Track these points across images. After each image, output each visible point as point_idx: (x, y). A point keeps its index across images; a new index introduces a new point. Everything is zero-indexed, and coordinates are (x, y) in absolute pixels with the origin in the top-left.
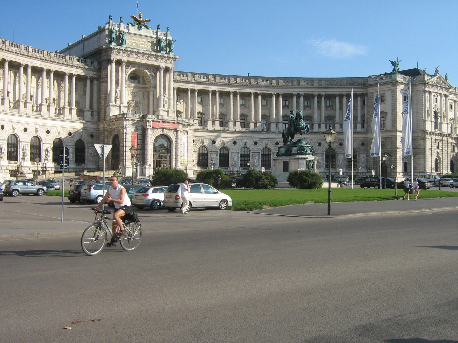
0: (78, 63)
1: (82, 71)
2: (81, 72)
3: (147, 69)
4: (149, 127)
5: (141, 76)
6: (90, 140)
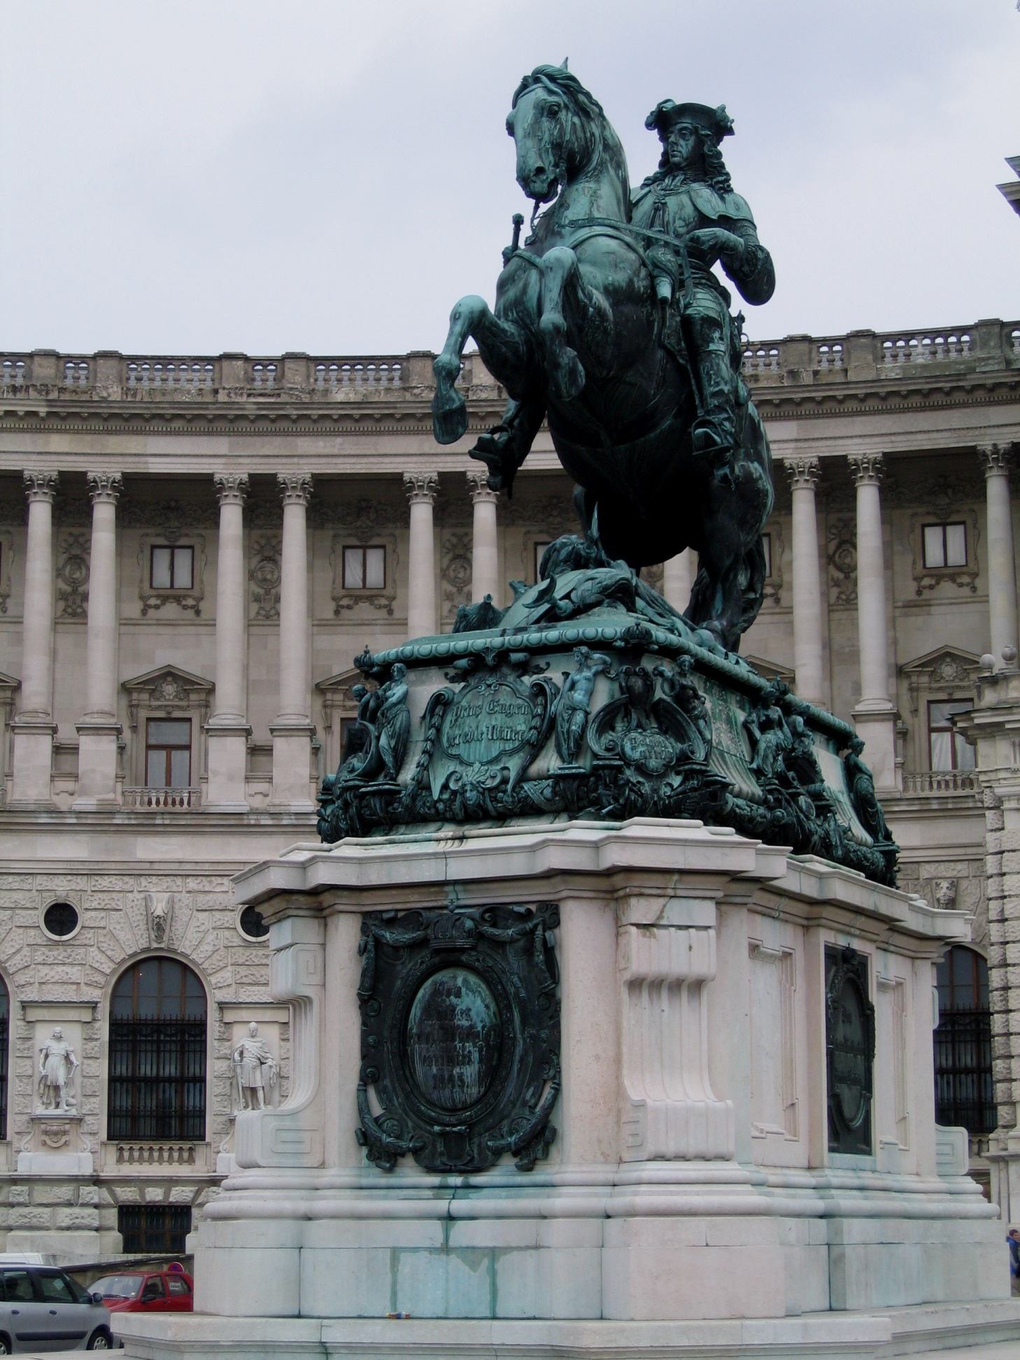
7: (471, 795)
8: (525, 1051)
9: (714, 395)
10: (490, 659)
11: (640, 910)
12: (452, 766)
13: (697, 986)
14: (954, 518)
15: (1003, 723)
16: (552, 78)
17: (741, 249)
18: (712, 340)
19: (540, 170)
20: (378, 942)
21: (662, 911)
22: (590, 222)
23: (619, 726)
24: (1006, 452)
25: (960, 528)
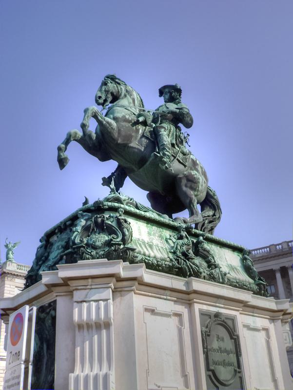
8: (48, 360)
9: (161, 146)
10: (62, 227)
11: (78, 295)
17: (178, 112)
18: (161, 131)
19: (100, 97)
21: (87, 295)
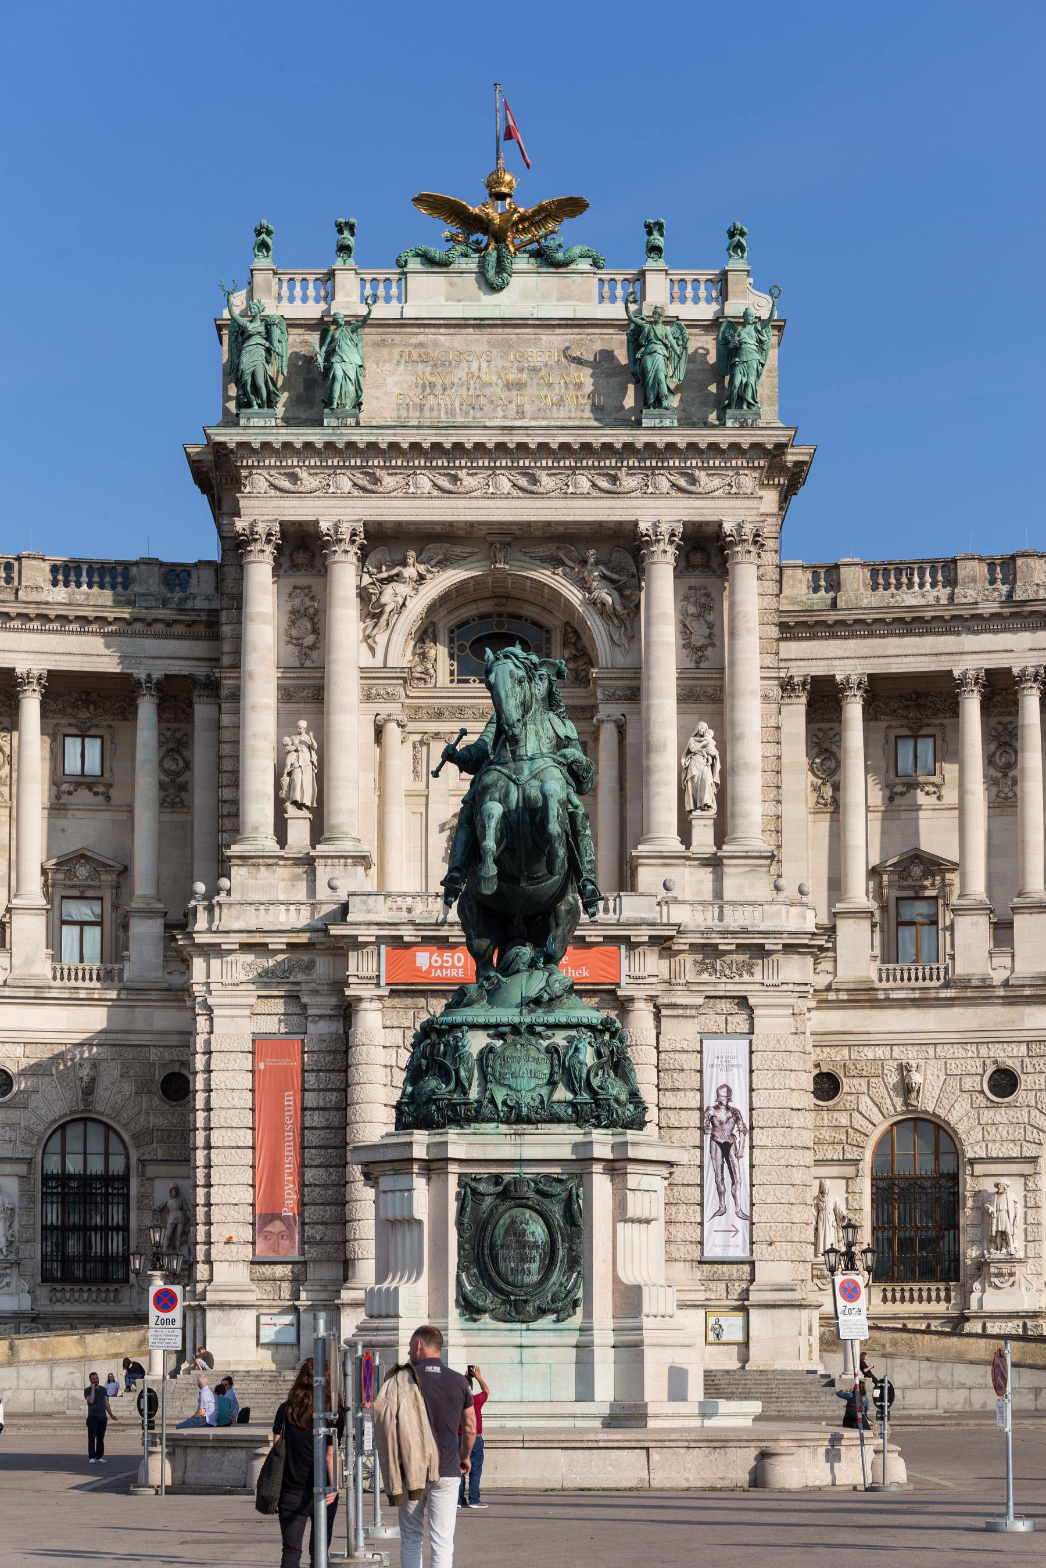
0: (60, 594)
1: (97, 643)
2: (92, 654)
3: (555, 562)
4: (367, 992)
5: (555, 623)
6: (155, 1121)
7: (525, 1110)
10: (523, 1029)
11: (632, 1181)
12: (505, 1091)
13: (648, 1222)
14: (92, 732)
15: (219, 945)
16: (517, 658)
20: (474, 1191)
22: (542, 755)
23: (600, 1073)
24: (158, 683)
25: (98, 742)
